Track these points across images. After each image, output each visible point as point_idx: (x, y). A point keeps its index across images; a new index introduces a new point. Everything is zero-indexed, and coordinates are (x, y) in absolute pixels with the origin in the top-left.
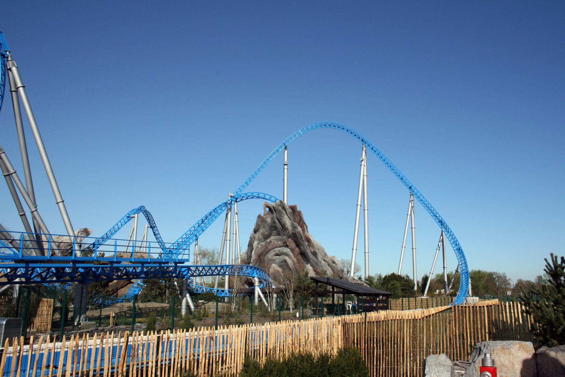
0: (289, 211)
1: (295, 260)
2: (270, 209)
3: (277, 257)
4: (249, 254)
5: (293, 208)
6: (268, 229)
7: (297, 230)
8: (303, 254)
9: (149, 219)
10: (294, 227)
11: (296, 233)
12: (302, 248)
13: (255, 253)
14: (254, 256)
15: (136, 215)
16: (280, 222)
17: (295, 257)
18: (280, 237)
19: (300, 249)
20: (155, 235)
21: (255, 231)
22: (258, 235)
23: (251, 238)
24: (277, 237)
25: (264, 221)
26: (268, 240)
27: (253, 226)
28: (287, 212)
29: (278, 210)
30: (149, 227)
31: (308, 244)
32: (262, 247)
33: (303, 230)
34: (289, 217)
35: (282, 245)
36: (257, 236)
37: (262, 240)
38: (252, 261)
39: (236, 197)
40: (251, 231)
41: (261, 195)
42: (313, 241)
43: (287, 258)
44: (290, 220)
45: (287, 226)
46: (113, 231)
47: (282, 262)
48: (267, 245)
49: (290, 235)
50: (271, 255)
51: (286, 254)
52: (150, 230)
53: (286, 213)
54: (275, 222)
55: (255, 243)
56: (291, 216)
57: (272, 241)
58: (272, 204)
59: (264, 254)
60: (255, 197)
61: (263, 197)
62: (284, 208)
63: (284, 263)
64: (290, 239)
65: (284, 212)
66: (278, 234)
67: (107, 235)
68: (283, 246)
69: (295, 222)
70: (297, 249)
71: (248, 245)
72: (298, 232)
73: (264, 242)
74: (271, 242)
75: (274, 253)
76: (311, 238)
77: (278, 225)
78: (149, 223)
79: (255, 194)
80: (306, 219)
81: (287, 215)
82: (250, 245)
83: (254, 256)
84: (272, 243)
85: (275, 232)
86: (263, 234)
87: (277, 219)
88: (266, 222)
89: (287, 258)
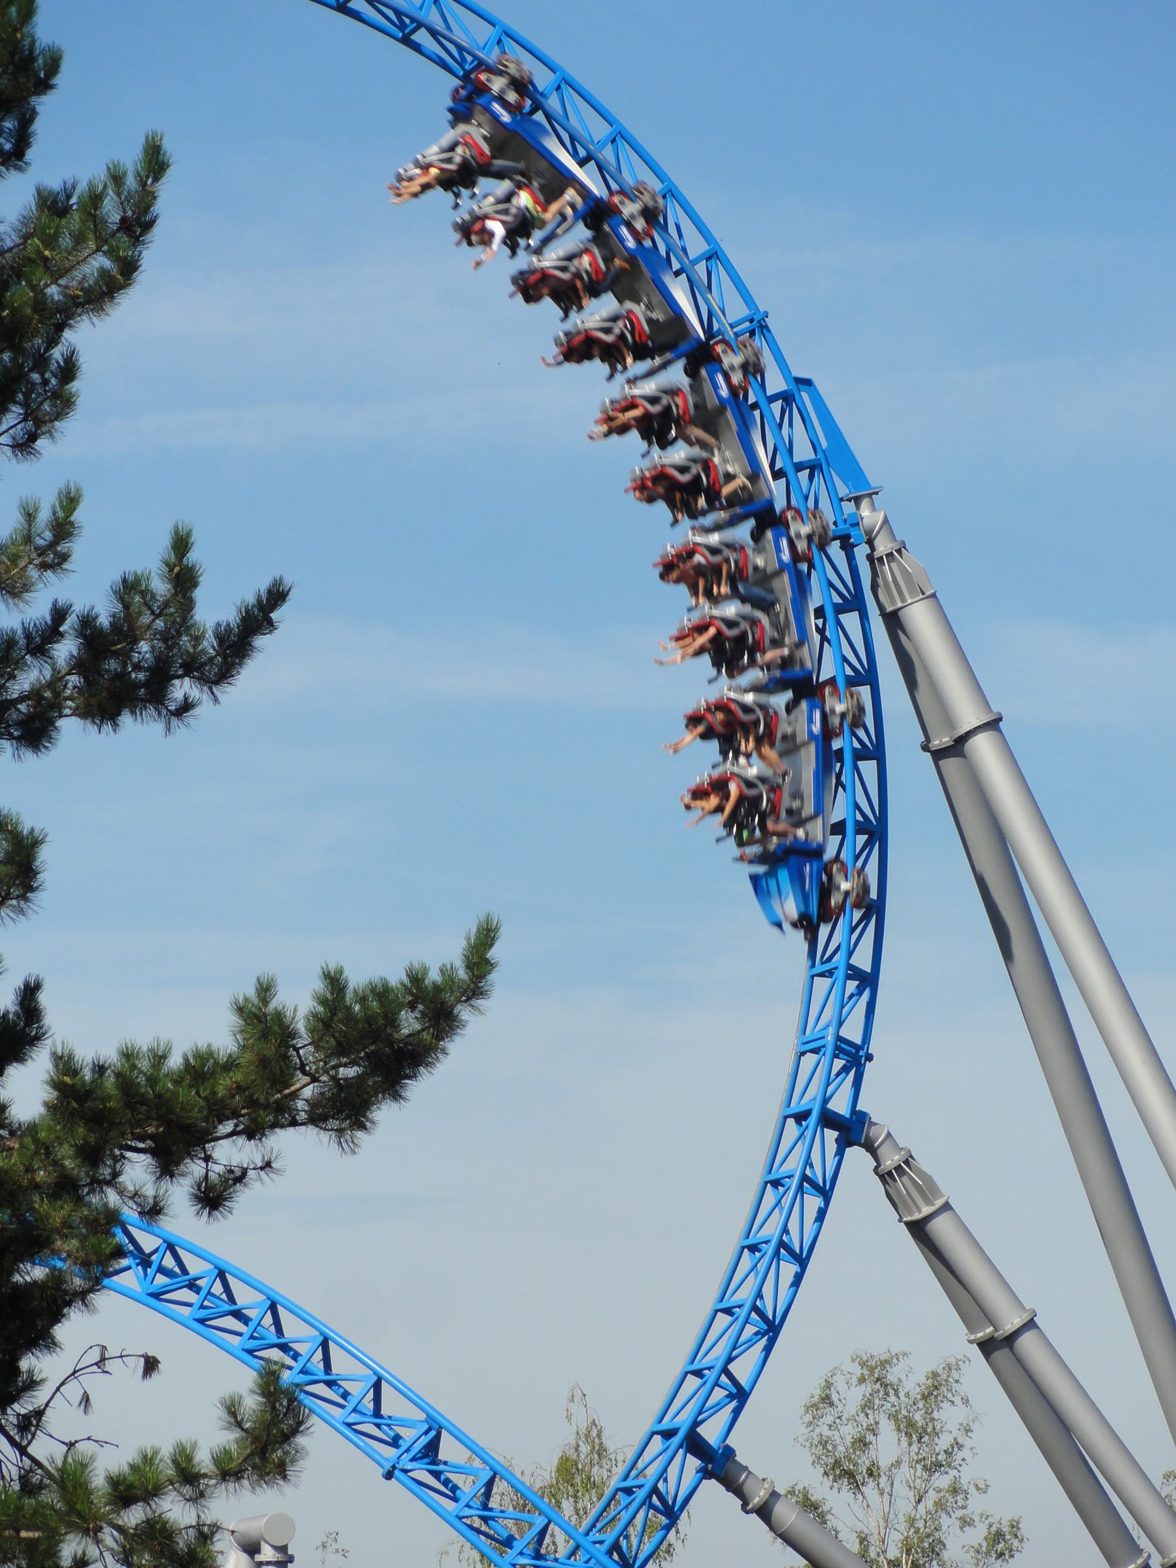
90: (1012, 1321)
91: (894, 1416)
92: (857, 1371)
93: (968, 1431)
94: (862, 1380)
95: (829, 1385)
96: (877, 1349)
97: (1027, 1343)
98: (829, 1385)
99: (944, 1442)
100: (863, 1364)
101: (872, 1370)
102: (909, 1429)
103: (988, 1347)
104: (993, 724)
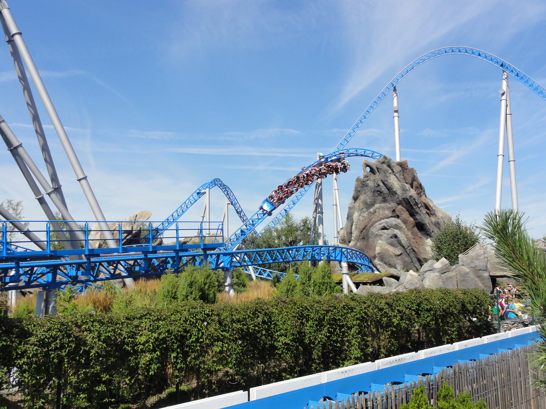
0: (397, 169)
1: (409, 233)
2: (372, 171)
3: (385, 231)
4: (349, 230)
5: (403, 165)
6: (370, 194)
7: (410, 195)
8: (421, 227)
9: (228, 194)
10: (404, 190)
11: (408, 198)
12: (417, 217)
13: (356, 228)
14: (355, 233)
15: (207, 189)
16: (385, 185)
17: (408, 229)
18: (387, 204)
19: (415, 219)
20: (238, 212)
21: (355, 199)
22: (358, 205)
23: (350, 208)
24: (382, 205)
25: (364, 185)
26: (371, 210)
27: (352, 193)
28: (394, 170)
29: (381, 169)
30: (229, 204)
31: (427, 212)
32: (365, 219)
33: (419, 194)
34: (397, 178)
35: (390, 215)
37: (364, 210)
38: (353, 239)
39: (326, 157)
40: (350, 200)
41: (359, 152)
42: (434, 208)
43: (397, 232)
44: (400, 181)
45: (394, 190)
46: (181, 212)
47: (391, 237)
48: (371, 216)
49: (400, 201)
50: (375, 229)
51: (396, 227)
52: (231, 206)
53: (393, 172)
54: (379, 185)
55: (356, 215)
56: (400, 175)
57: (377, 210)
58: (372, 162)
59: (367, 228)
60: (351, 155)
61: (363, 153)
62: (389, 166)
63: (394, 239)
64: (400, 206)
65: (391, 171)
66: (385, 200)
67: (173, 216)
68: (392, 217)
69: (406, 183)
70: (412, 219)
71: (347, 218)
72: (410, 196)
73: (367, 213)
74: (375, 212)
75: (381, 226)
76: (431, 205)
77: (384, 189)
78: (229, 198)
79: (351, 151)
80: (422, 177)
81: (395, 175)
82: (350, 217)
83: (355, 233)
84: (377, 214)
85: (380, 198)
86: (365, 203)
87: (383, 183)
88: (367, 186)
89: (397, 232)
90: (16, 144)
91: (12, 208)
92: (7, 202)
93: (22, 210)
94: (8, 203)
95: (2, 203)
96: (10, 199)
97: (20, 150)
98: (2, 203)
99: (19, 211)
100: (8, 201)
101: (9, 201)
102: (14, 209)
103: (11, 150)
104: (20, 34)
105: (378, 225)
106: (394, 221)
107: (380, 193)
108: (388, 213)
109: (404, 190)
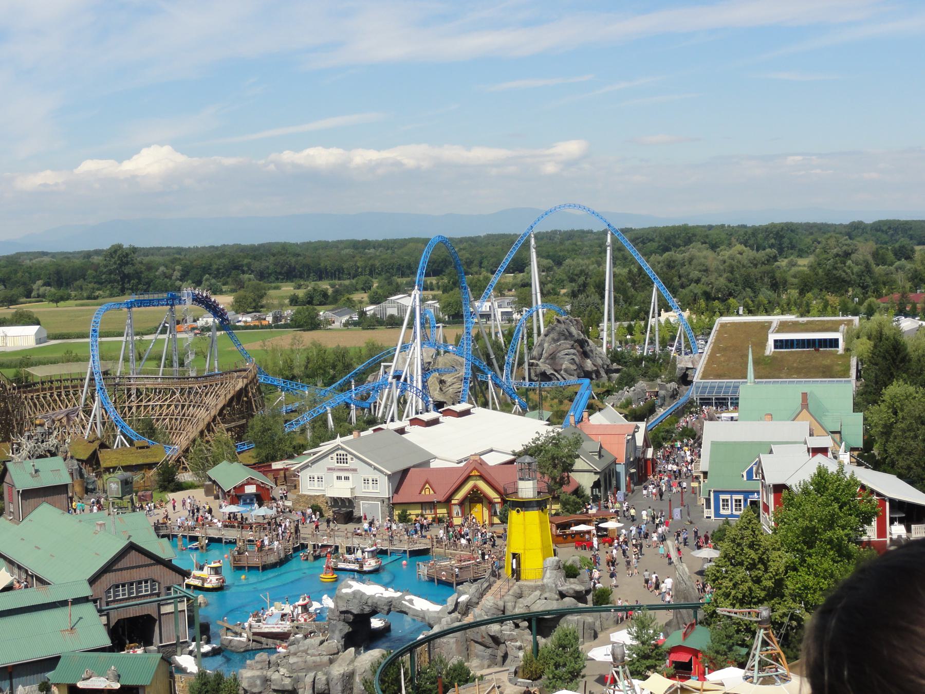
36: (547, 339)
43: (574, 357)
50: (561, 354)
51: (574, 354)
55: (546, 345)
66: (566, 339)
77: (567, 333)
83: (545, 355)
85: (563, 337)
105: (563, 353)
106: (572, 351)
107: (564, 335)
108: (568, 346)
109: (579, 335)
